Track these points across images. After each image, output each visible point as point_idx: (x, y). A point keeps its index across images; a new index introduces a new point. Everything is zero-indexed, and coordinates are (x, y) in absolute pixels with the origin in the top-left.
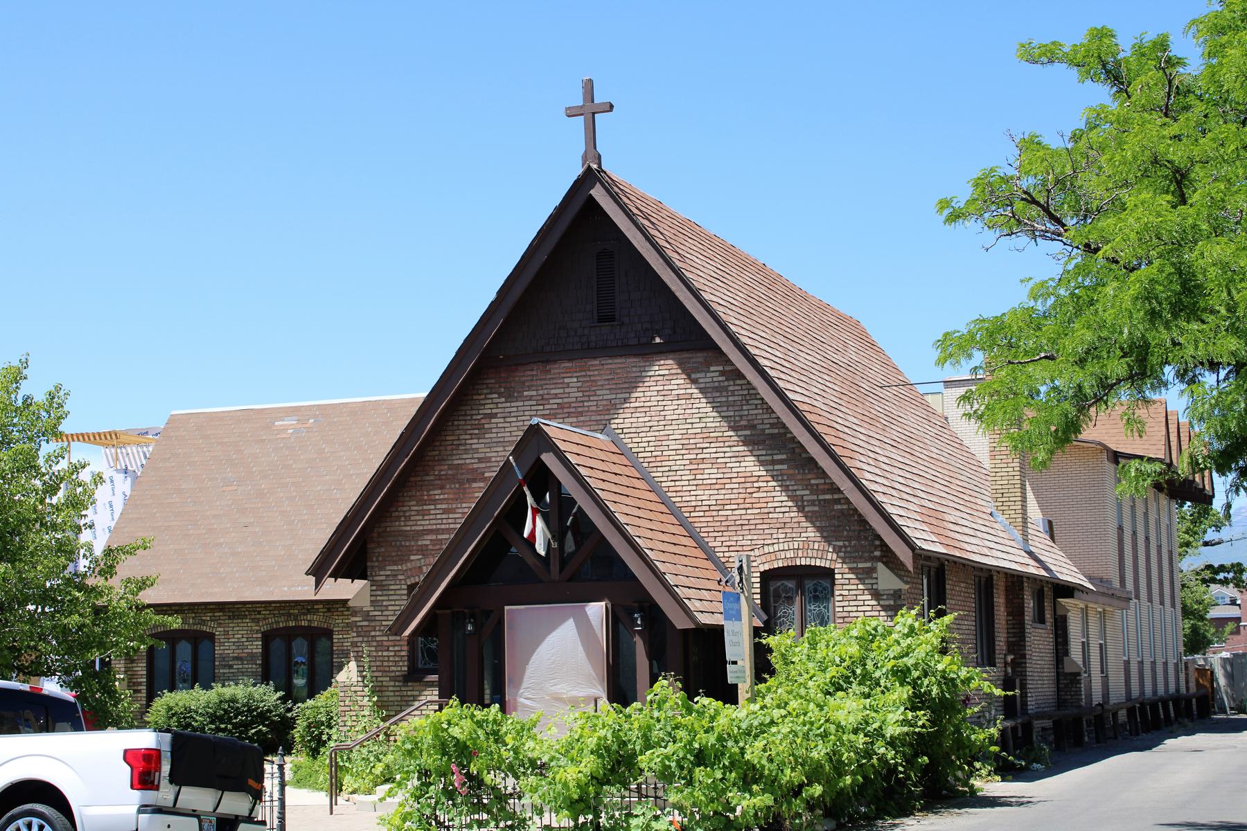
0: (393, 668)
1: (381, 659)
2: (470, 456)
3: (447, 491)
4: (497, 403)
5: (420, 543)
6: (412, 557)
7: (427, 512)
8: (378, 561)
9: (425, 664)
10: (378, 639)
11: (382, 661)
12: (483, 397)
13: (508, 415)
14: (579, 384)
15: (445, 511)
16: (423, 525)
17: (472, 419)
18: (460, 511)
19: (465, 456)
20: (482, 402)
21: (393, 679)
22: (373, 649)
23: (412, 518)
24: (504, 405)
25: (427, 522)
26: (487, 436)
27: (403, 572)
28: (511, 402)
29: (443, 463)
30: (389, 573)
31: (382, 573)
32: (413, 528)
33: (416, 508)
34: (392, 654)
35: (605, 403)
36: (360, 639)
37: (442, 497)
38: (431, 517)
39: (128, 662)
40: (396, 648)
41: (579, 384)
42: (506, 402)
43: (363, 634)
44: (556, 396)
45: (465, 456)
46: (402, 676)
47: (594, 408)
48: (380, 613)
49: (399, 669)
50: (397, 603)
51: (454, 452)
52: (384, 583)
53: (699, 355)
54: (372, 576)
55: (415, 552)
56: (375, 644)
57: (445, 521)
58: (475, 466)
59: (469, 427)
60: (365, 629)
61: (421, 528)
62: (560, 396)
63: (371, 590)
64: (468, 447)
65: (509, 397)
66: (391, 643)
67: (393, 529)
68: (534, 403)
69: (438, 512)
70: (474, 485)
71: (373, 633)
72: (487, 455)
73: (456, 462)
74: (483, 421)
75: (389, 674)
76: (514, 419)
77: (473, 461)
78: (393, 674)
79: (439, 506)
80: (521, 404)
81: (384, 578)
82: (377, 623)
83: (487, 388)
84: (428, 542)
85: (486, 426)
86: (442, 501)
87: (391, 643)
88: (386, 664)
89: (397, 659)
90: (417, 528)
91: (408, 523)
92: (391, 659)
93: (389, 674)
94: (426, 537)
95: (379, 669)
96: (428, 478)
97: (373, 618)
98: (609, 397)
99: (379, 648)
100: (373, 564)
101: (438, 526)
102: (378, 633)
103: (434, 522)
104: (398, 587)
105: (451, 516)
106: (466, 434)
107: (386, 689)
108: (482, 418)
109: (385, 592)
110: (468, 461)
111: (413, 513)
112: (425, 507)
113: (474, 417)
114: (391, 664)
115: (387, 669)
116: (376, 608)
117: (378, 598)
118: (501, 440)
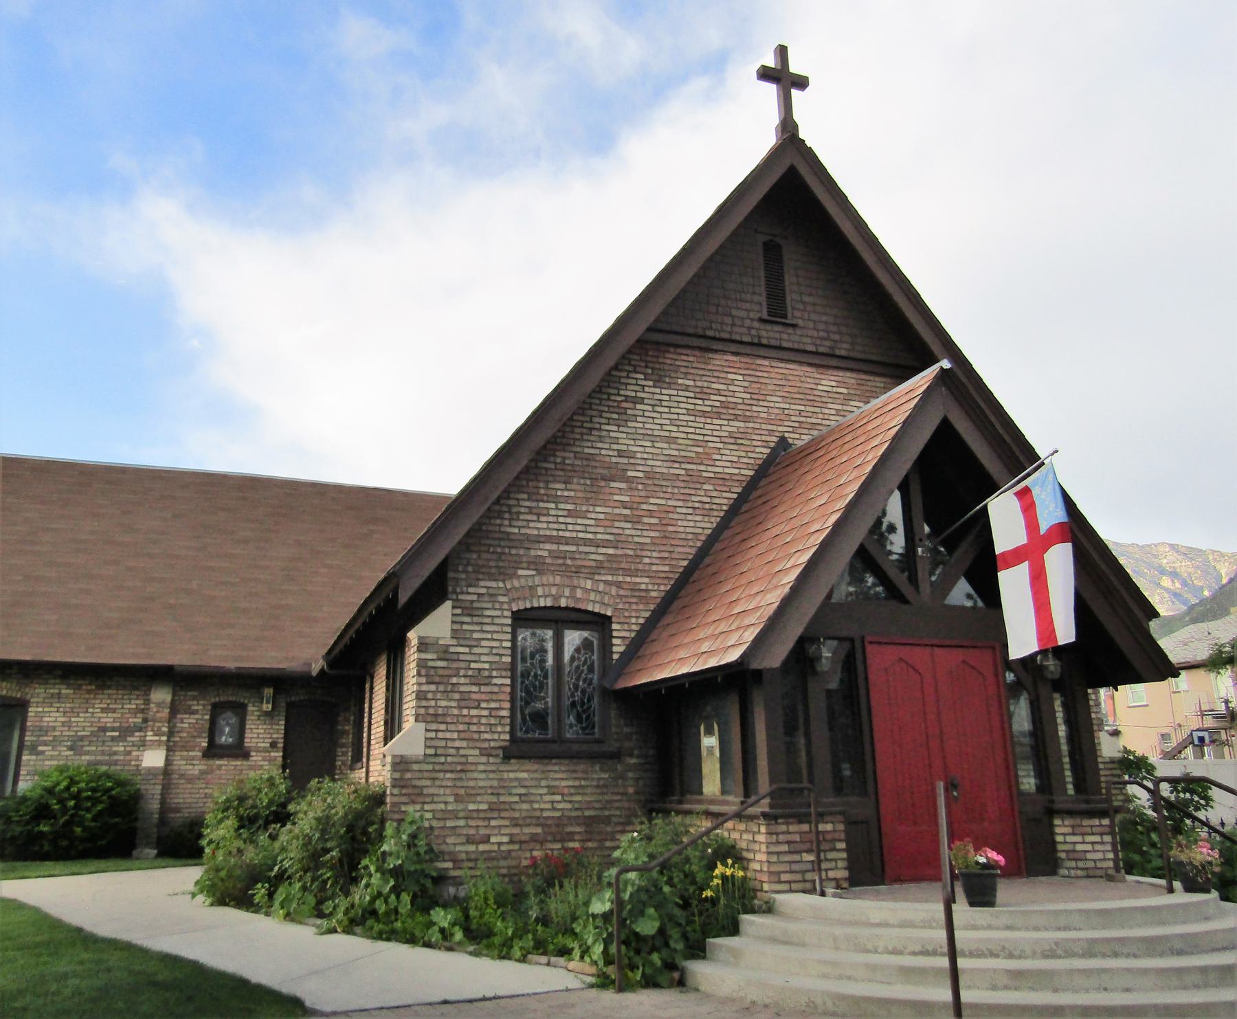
0: (487, 736)
1: (467, 720)
2: (607, 446)
3: (573, 487)
4: (644, 386)
5: (533, 553)
6: (520, 572)
7: (545, 512)
8: (465, 572)
9: (527, 732)
10: (462, 689)
11: (469, 724)
12: (624, 374)
13: (658, 403)
14: (746, 384)
15: (570, 514)
16: (538, 529)
17: (609, 399)
18: (593, 516)
19: (600, 445)
20: (623, 380)
21: (485, 752)
22: (453, 704)
23: (522, 517)
24: (652, 390)
25: (545, 525)
26: (630, 424)
27: (508, 592)
28: (661, 388)
29: (568, 448)
30: (484, 591)
31: (471, 590)
32: (523, 531)
33: (527, 504)
34: (485, 713)
35: (777, 411)
36: (433, 687)
37: (566, 494)
38: (551, 519)
39: (423, 680)
40: (493, 705)
41: (746, 384)
42: (654, 386)
43: (437, 679)
44: (719, 392)
45: (600, 445)
46: (500, 747)
47: (764, 415)
48: (467, 650)
49: (496, 737)
50: (495, 636)
51: (585, 437)
52: (475, 605)
53: (877, 379)
54: (454, 592)
55: (524, 565)
56: (457, 696)
57: (570, 527)
58: (614, 460)
59: (606, 409)
60: (441, 672)
61: (536, 532)
62: (723, 393)
63: (453, 615)
64: (604, 433)
65: (659, 382)
66: (483, 697)
67: (490, 528)
68: (692, 395)
69: (560, 513)
70: (613, 484)
71: (454, 680)
72: (631, 448)
73: (587, 450)
74: (624, 405)
75: (479, 744)
76: (666, 410)
77: (611, 453)
78: (486, 745)
79: (561, 506)
80: (675, 393)
81: (475, 597)
82: (463, 665)
83: (630, 364)
84: (546, 554)
85: (629, 412)
86: (567, 500)
87: (483, 697)
88: (474, 728)
89: (493, 721)
90: (528, 531)
91: (514, 523)
92: (484, 721)
93: (479, 744)
94: (542, 546)
95: (462, 735)
96: (546, 465)
97: (455, 657)
98: (782, 406)
99: (463, 703)
100: (458, 575)
101: (561, 533)
102: (462, 680)
103: (556, 526)
104: (498, 613)
105: (579, 521)
106: (601, 417)
107: (473, 768)
108: (622, 401)
109: (476, 619)
110: (603, 452)
111: (523, 510)
112: (541, 505)
113: (613, 398)
114: (483, 728)
115: (476, 736)
116: (462, 642)
117: (465, 627)
118: (650, 432)
